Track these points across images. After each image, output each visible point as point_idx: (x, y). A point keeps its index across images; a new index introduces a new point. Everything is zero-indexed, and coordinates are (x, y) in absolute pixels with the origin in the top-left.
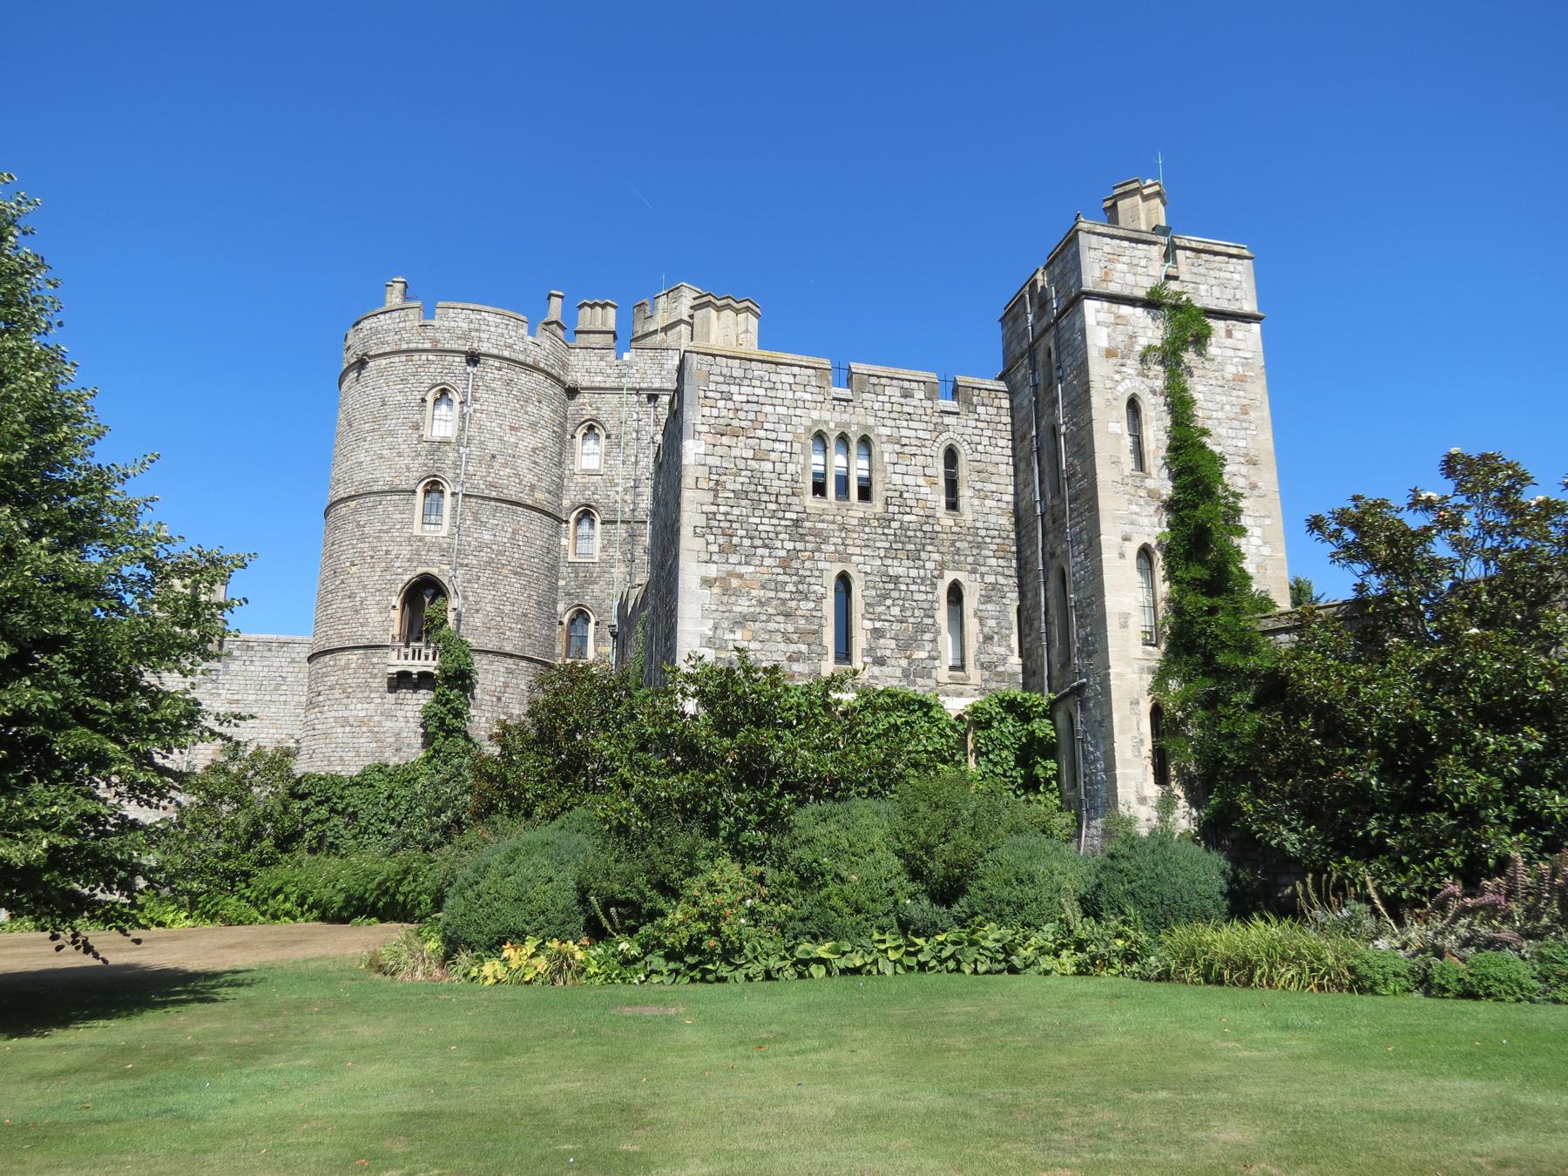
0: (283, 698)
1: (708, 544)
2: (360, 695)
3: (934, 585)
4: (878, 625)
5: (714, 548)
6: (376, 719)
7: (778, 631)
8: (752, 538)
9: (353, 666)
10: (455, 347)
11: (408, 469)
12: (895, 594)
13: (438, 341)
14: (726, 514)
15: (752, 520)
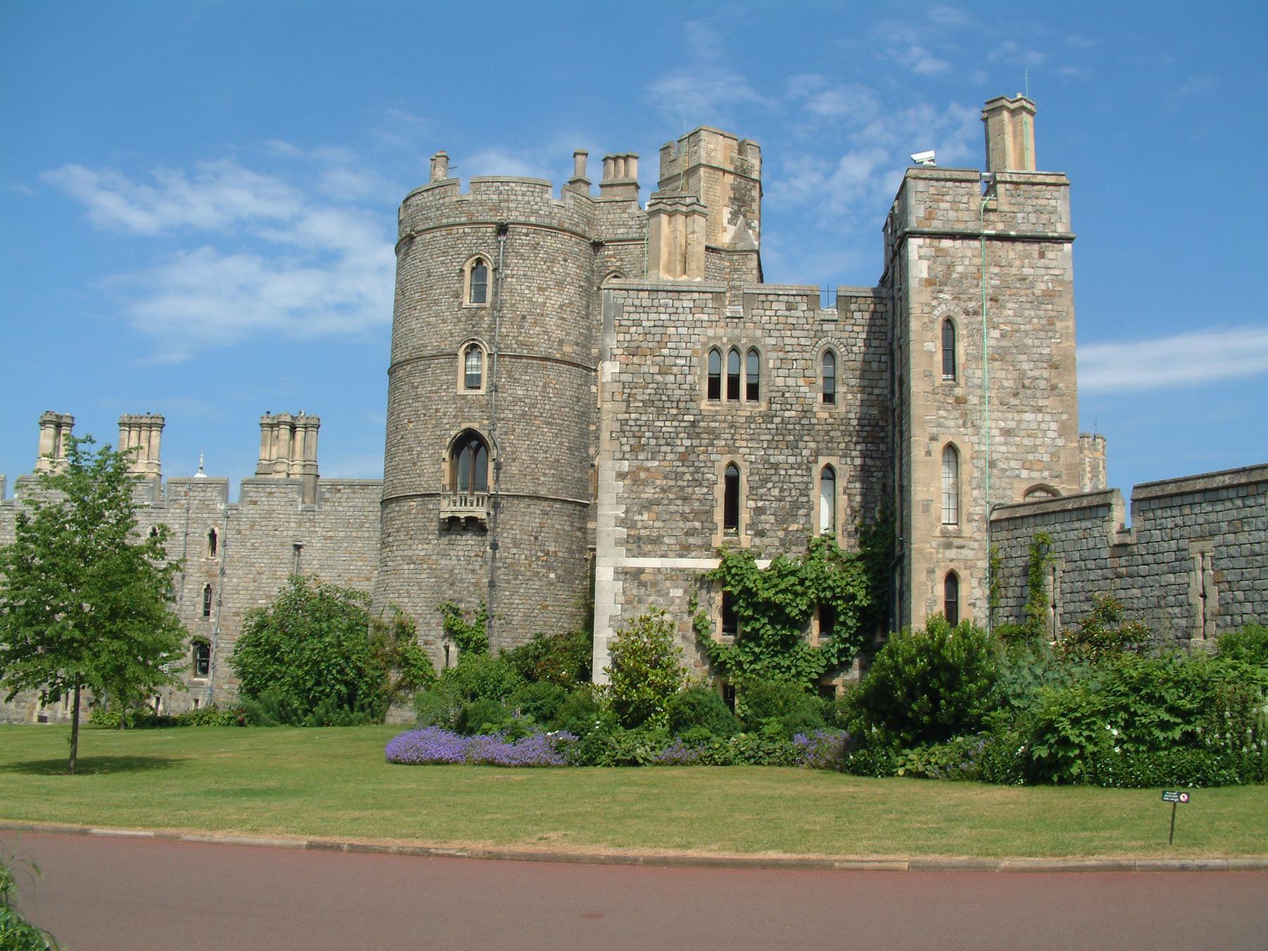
0: (366, 535)
1: (622, 445)
2: (420, 537)
3: (809, 469)
4: (760, 504)
5: (627, 448)
6: (434, 557)
7: (677, 512)
8: (657, 438)
9: (414, 511)
10: (488, 218)
11: (452, 335)
12: (775, 478)
13: (473, 215)
14: (636, 420)
15: (657, 423)
